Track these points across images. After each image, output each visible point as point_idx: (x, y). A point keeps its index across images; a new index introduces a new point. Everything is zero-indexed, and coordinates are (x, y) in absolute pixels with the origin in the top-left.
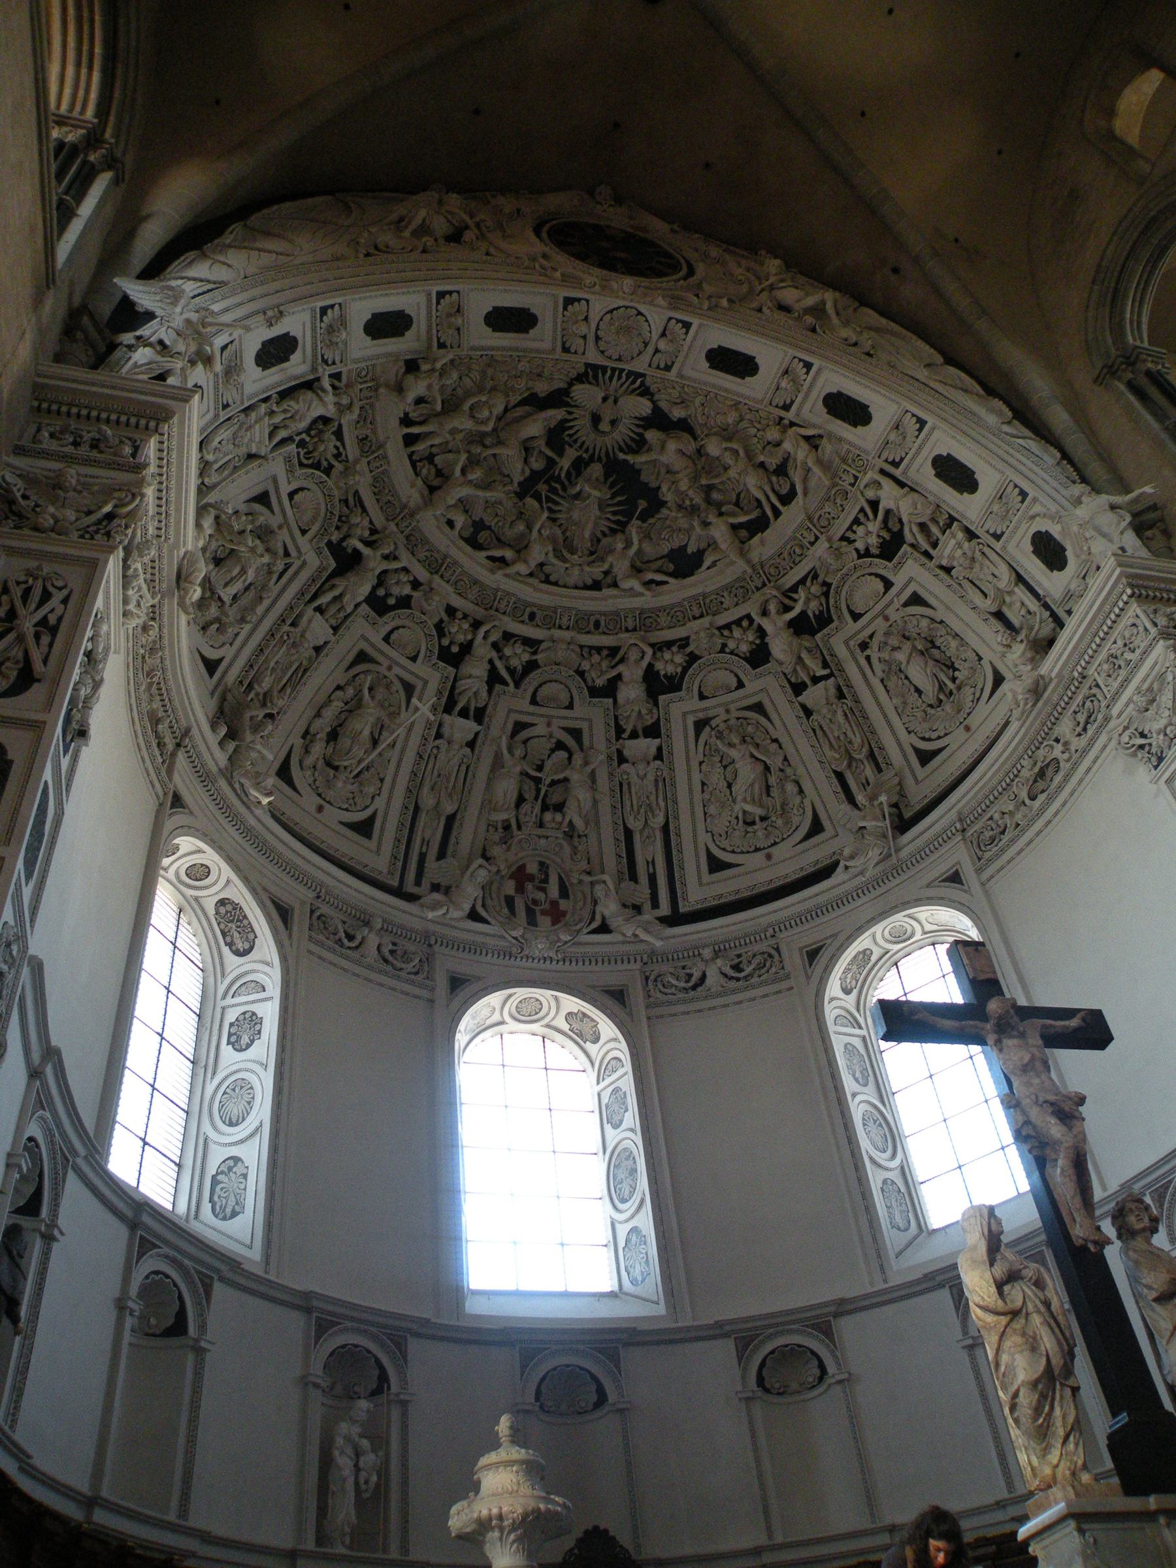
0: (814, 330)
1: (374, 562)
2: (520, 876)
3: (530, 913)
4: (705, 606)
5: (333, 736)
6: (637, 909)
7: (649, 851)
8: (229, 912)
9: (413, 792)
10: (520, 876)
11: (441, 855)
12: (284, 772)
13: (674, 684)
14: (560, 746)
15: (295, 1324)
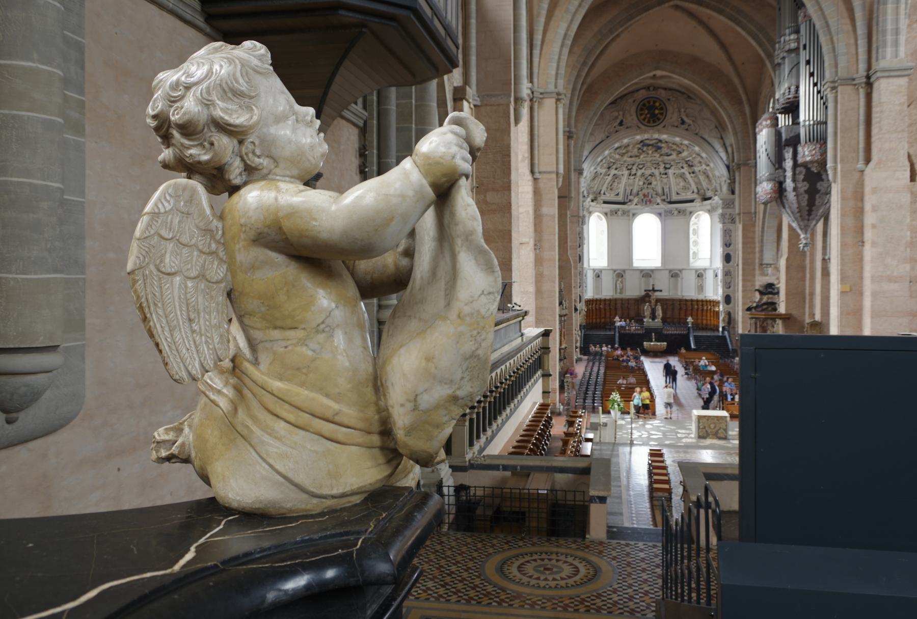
0: (687, 130)
1: (614, 167)
2: (644, 195)
3: (646, 202)
4: (674, 160)
5: (611, 185)
6: (664, 200)
7: (666, 190)
8: (599, 217)
9: (625, 186)
10: (644, 195)
11: (631, 195)
12: (604, 194)
13: (669, 168)
14: (650, 175)
15: (612, 272)
